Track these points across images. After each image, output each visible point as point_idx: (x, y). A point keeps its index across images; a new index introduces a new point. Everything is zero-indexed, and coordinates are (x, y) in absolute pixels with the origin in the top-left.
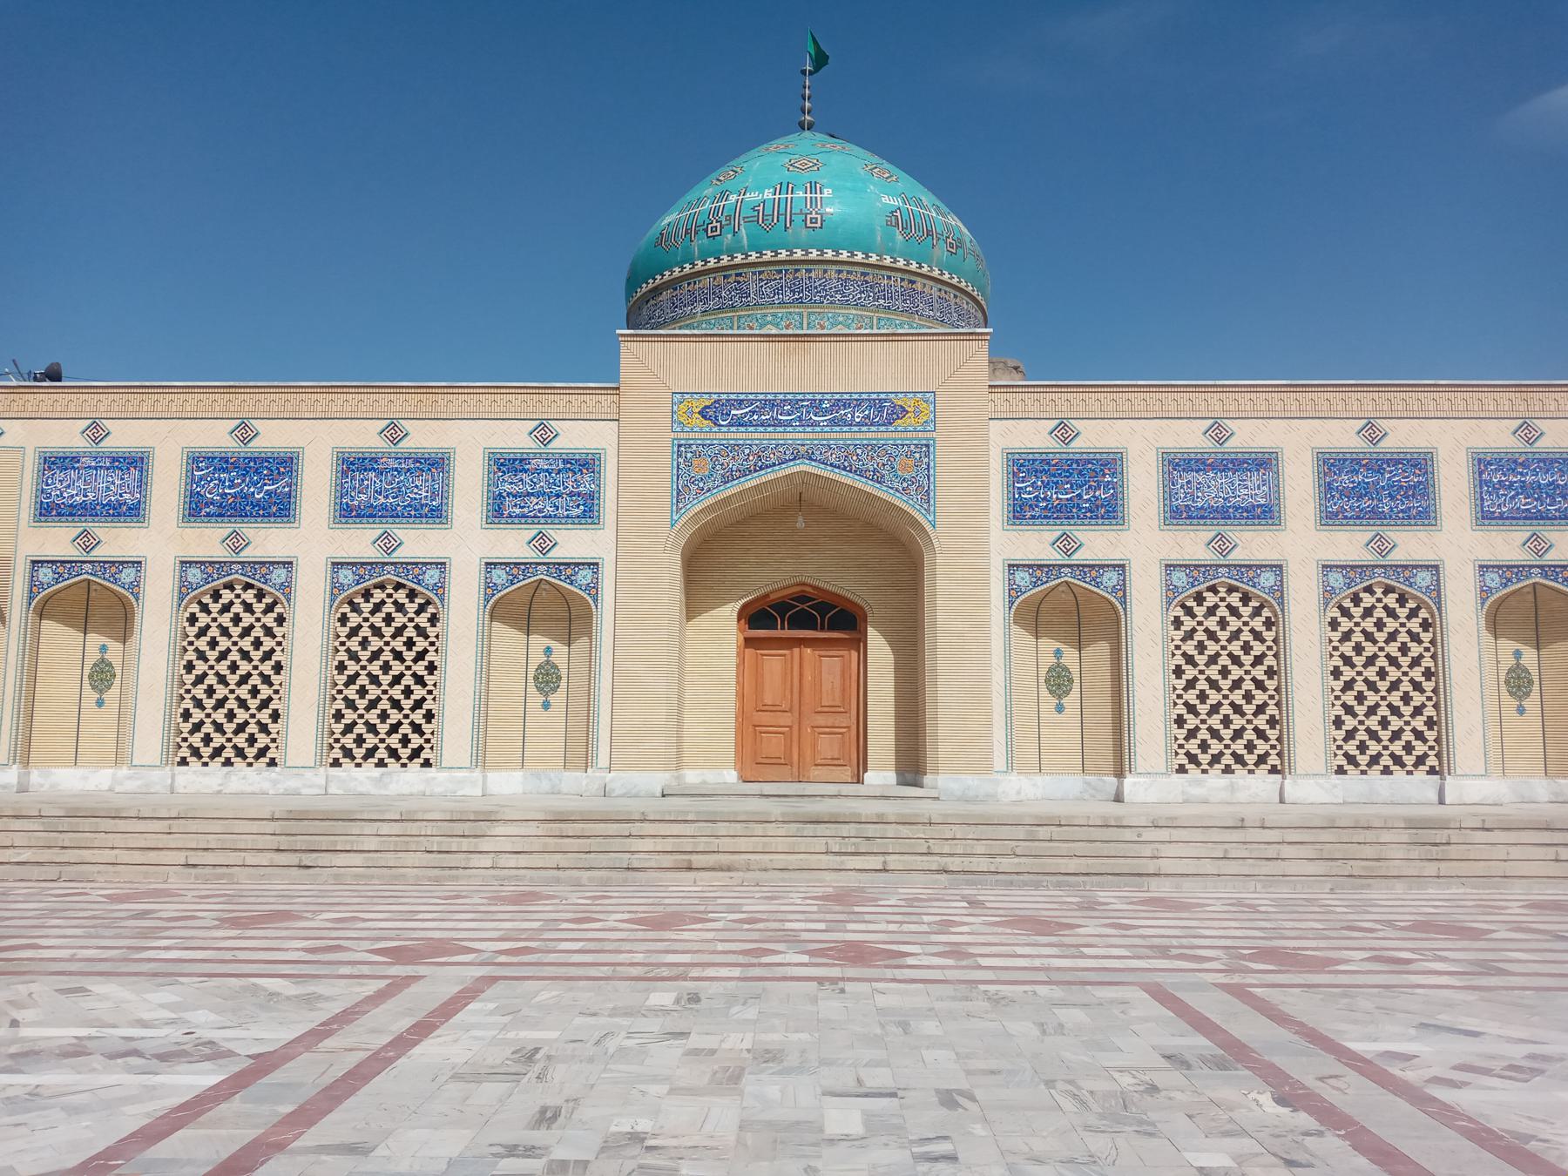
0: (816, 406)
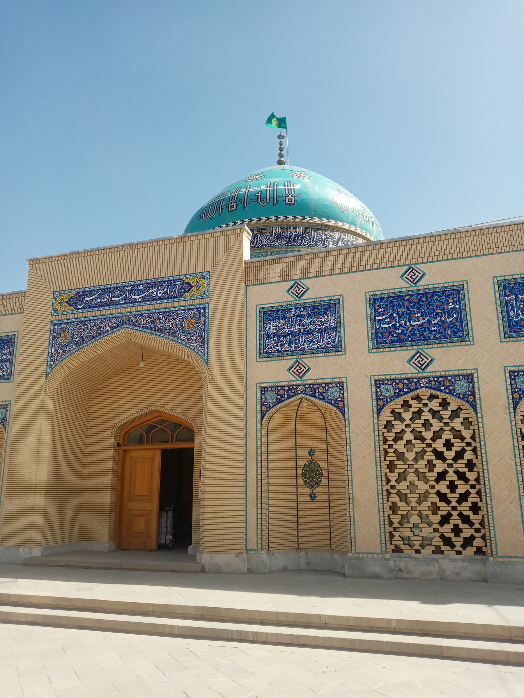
0: (135, 288)
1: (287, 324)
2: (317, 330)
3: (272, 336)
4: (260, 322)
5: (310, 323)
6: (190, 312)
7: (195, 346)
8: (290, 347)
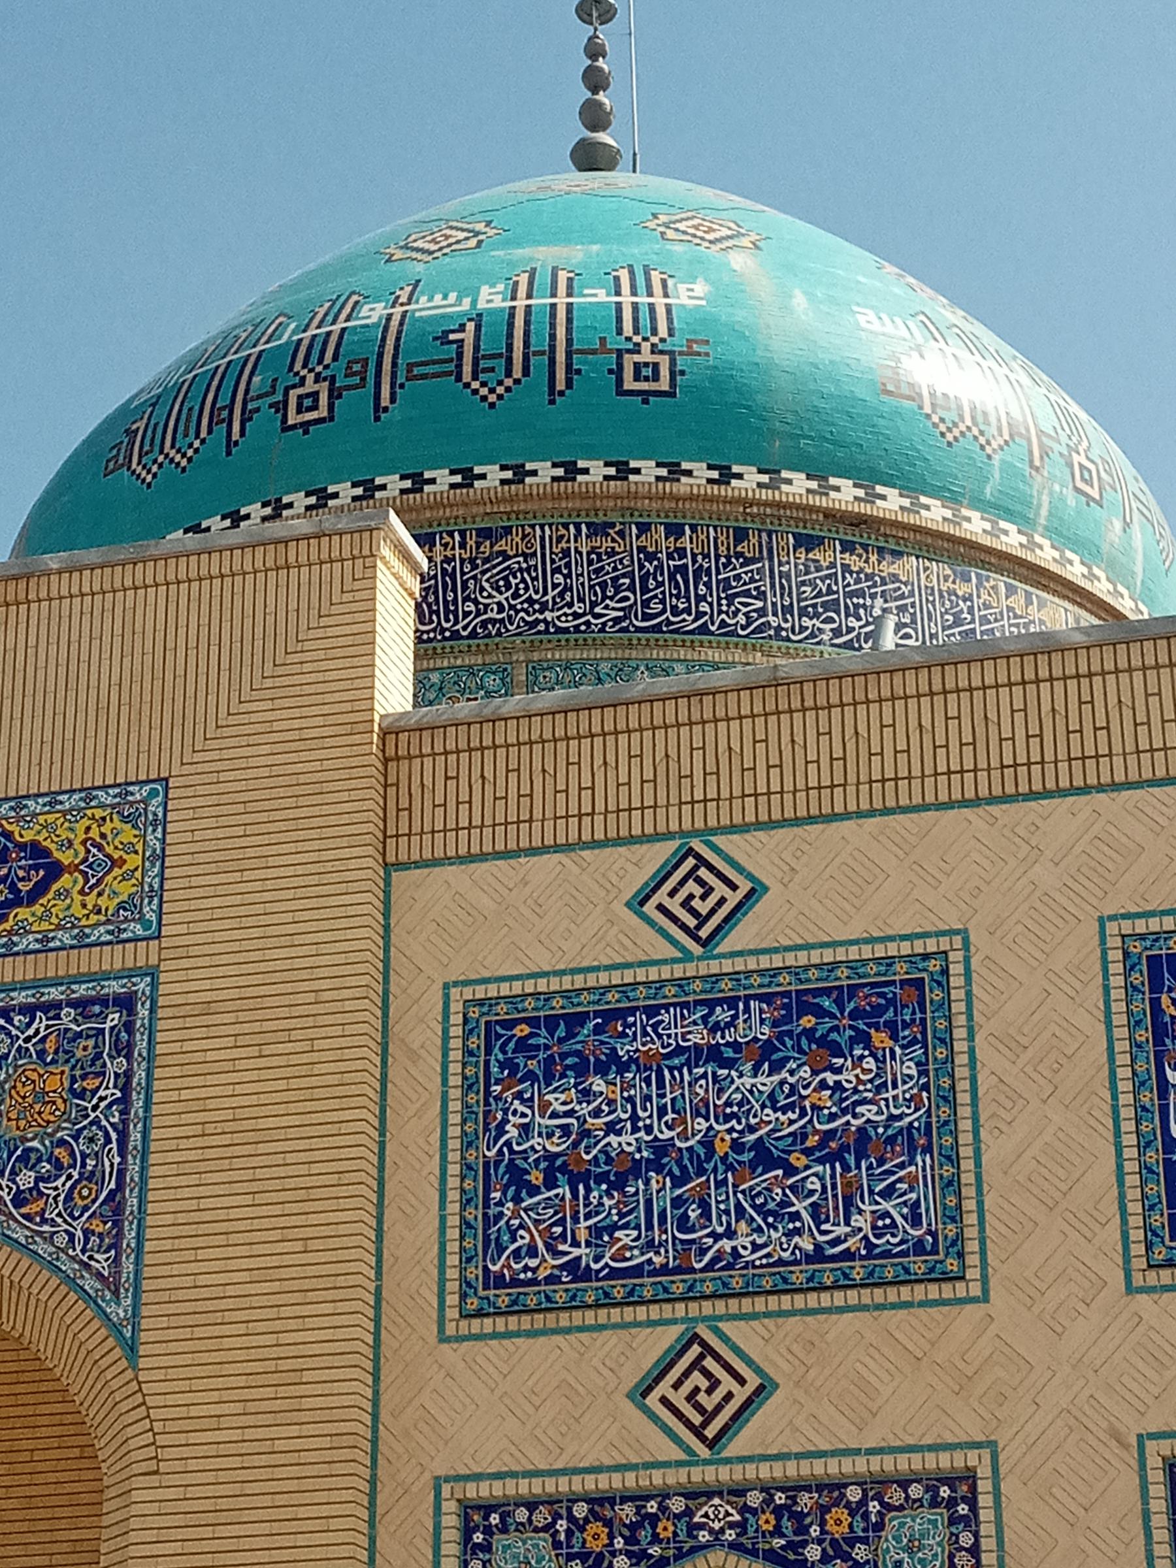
1: (630, 1100)
2: (813, 1140)
3: (536, 1177)
4: (468, 1086)
5: (772, 1096)
6: (41, 1023)
7: (61, 1240)
8: (650, 1244)
